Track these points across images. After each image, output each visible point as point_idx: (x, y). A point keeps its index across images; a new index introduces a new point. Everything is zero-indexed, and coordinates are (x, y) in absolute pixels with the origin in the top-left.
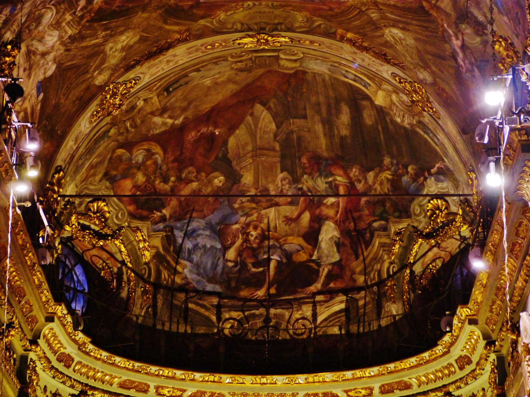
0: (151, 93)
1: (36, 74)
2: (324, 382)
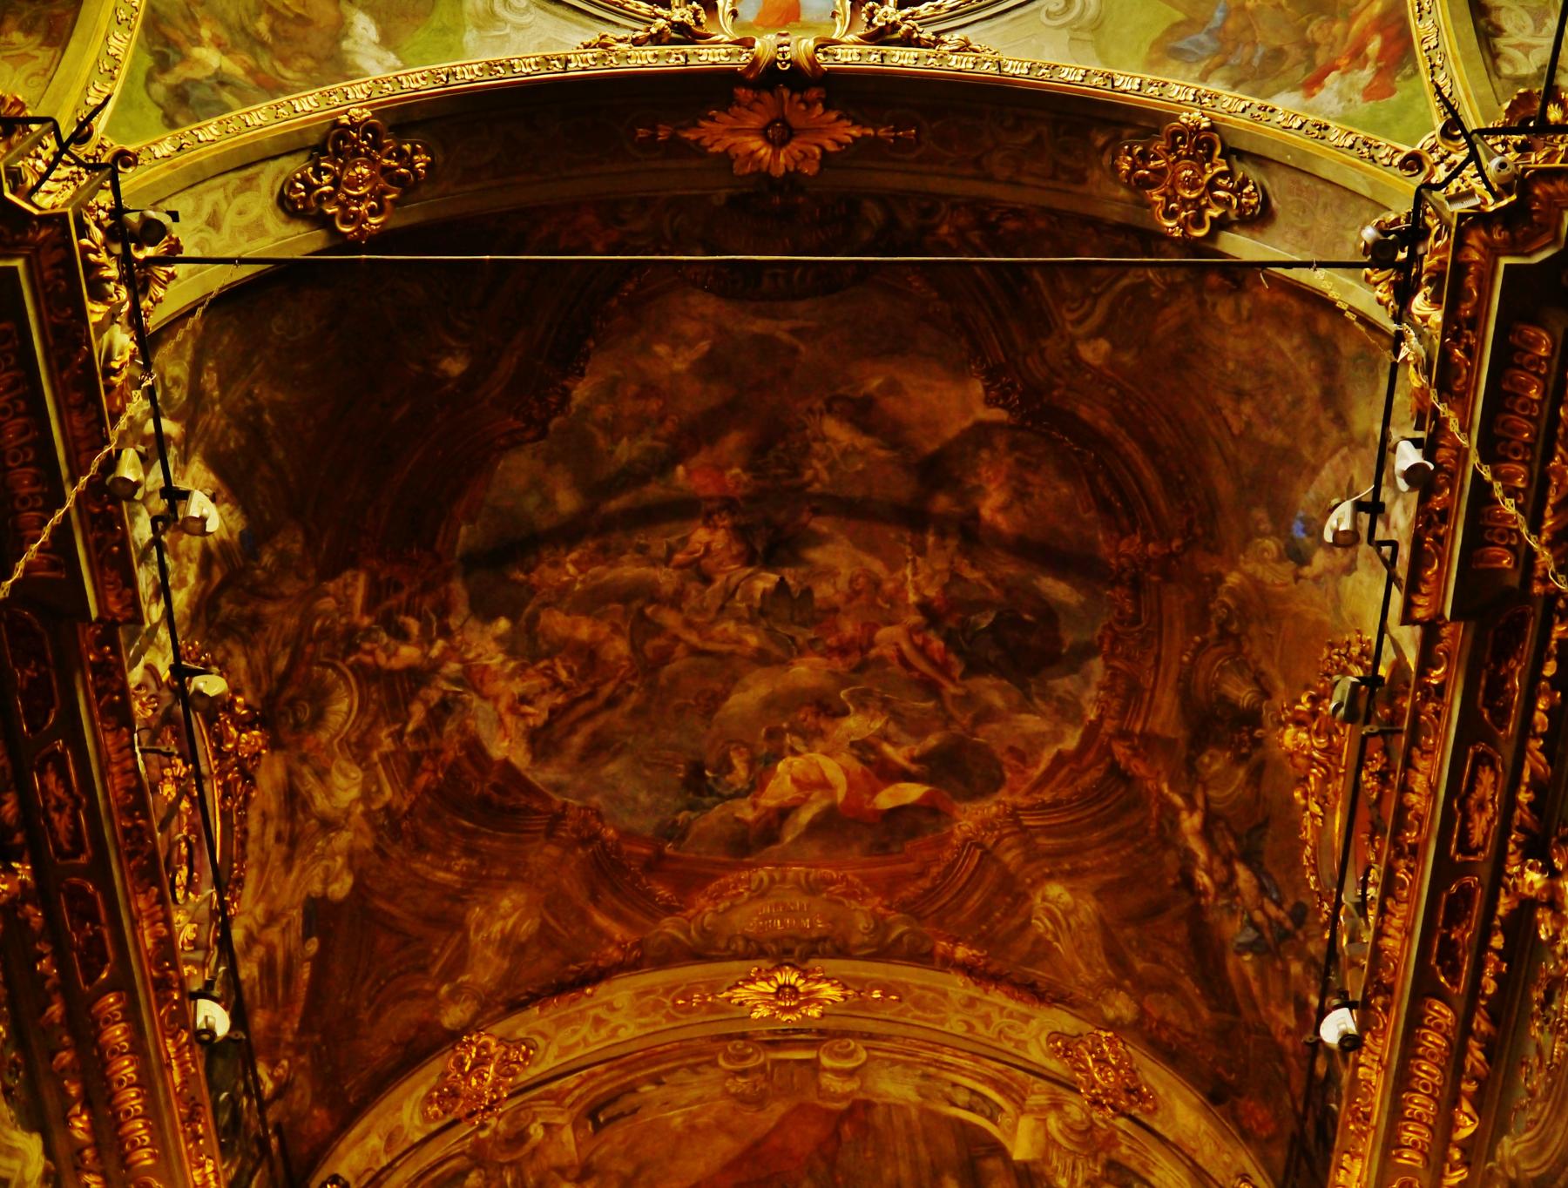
0: (561, 1113)
1: (303, 869)
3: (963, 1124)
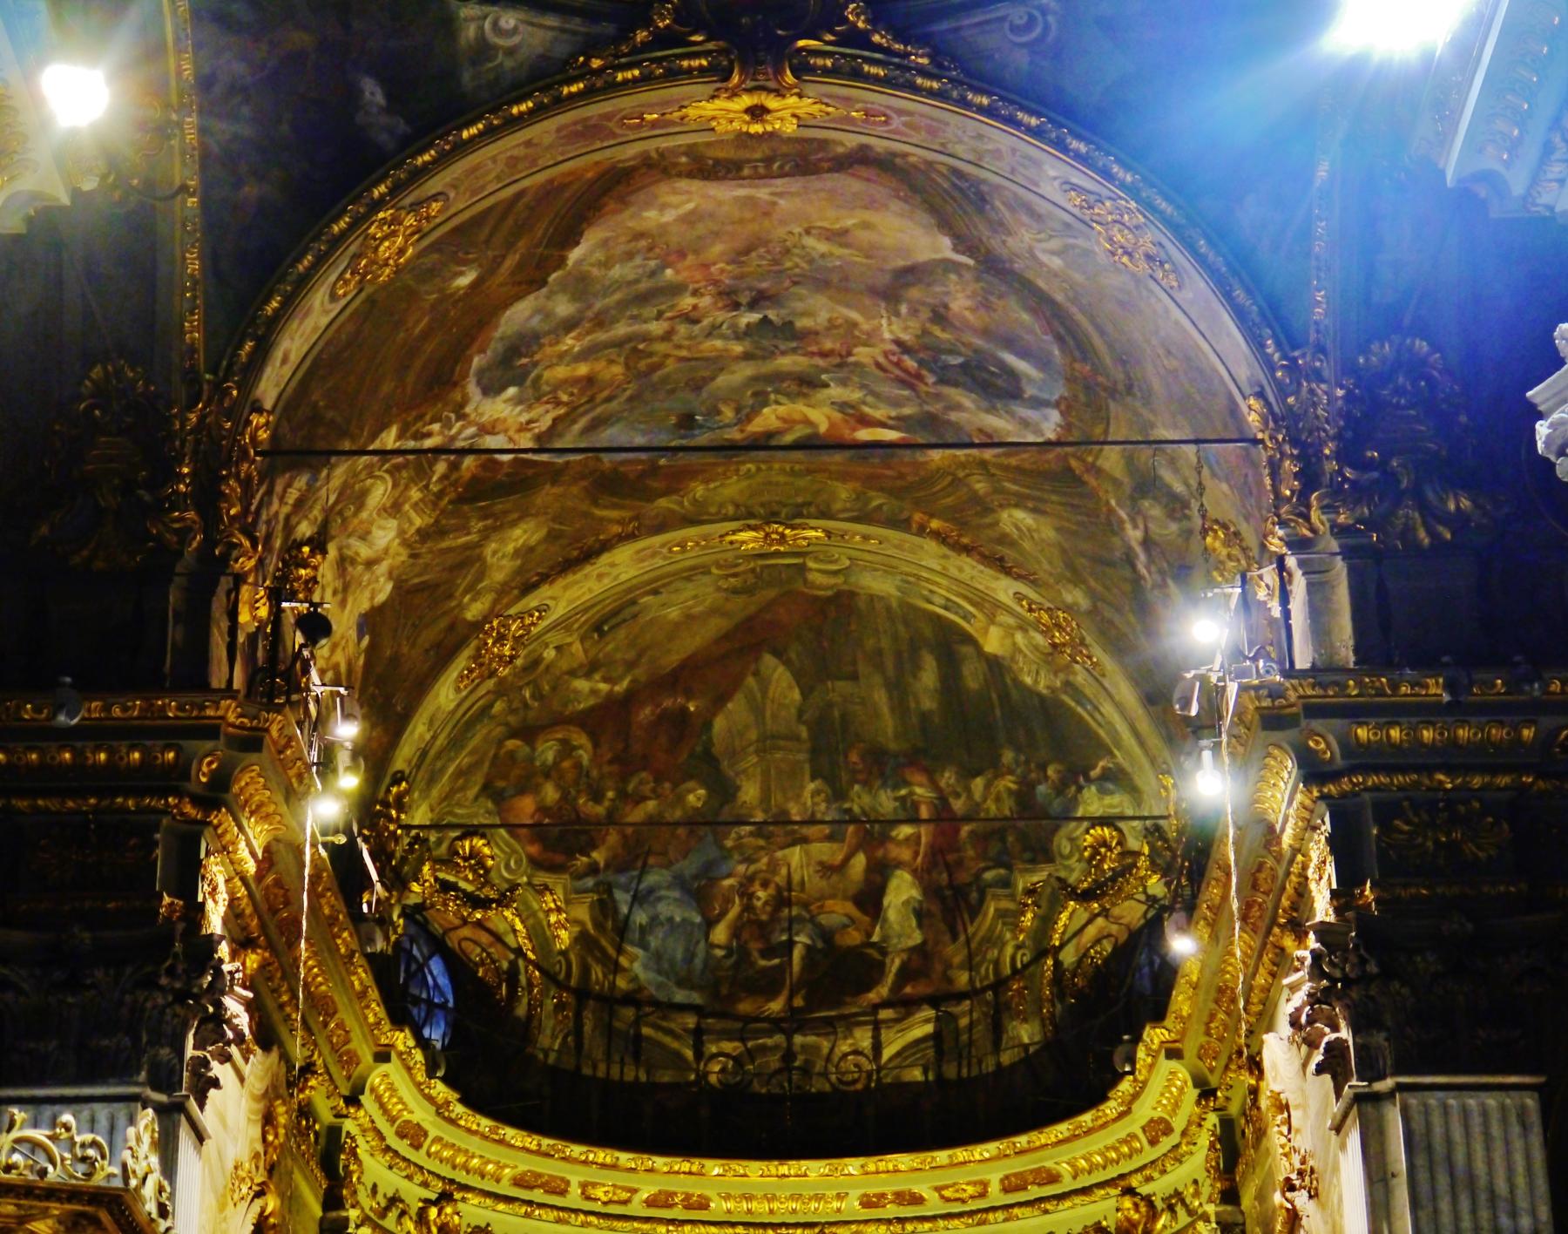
2: (897, 1171)
3: (939, 617)
